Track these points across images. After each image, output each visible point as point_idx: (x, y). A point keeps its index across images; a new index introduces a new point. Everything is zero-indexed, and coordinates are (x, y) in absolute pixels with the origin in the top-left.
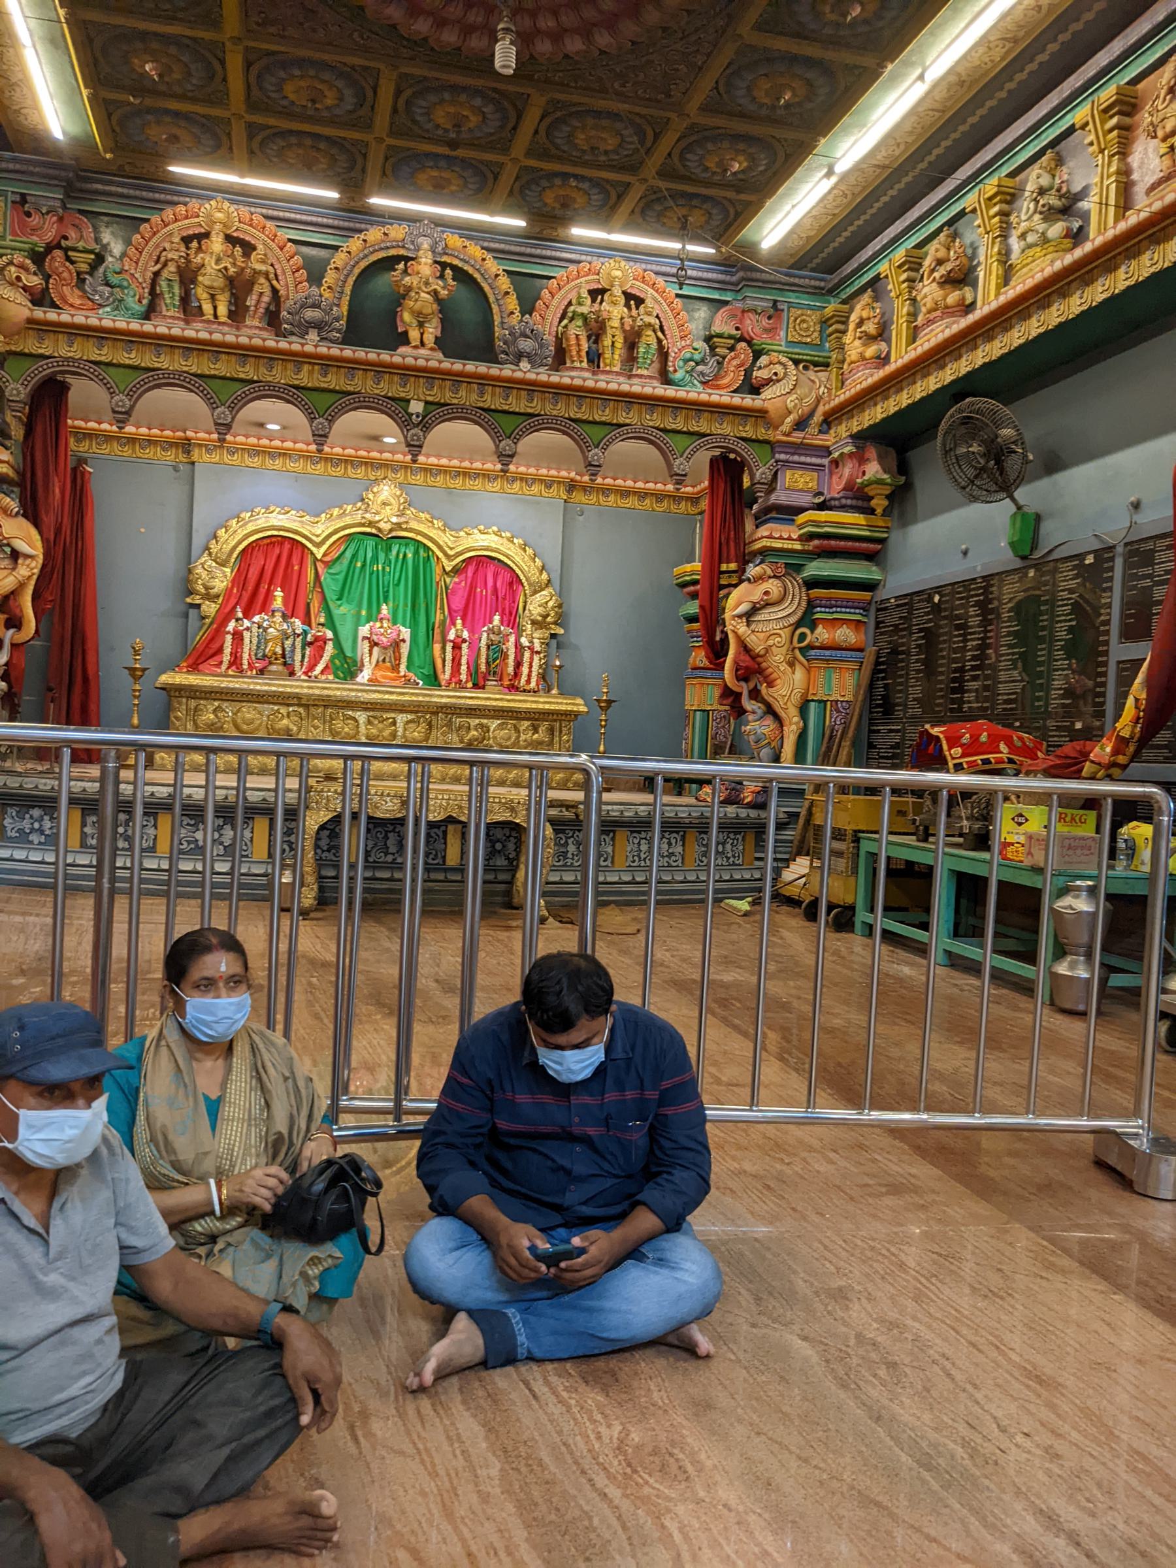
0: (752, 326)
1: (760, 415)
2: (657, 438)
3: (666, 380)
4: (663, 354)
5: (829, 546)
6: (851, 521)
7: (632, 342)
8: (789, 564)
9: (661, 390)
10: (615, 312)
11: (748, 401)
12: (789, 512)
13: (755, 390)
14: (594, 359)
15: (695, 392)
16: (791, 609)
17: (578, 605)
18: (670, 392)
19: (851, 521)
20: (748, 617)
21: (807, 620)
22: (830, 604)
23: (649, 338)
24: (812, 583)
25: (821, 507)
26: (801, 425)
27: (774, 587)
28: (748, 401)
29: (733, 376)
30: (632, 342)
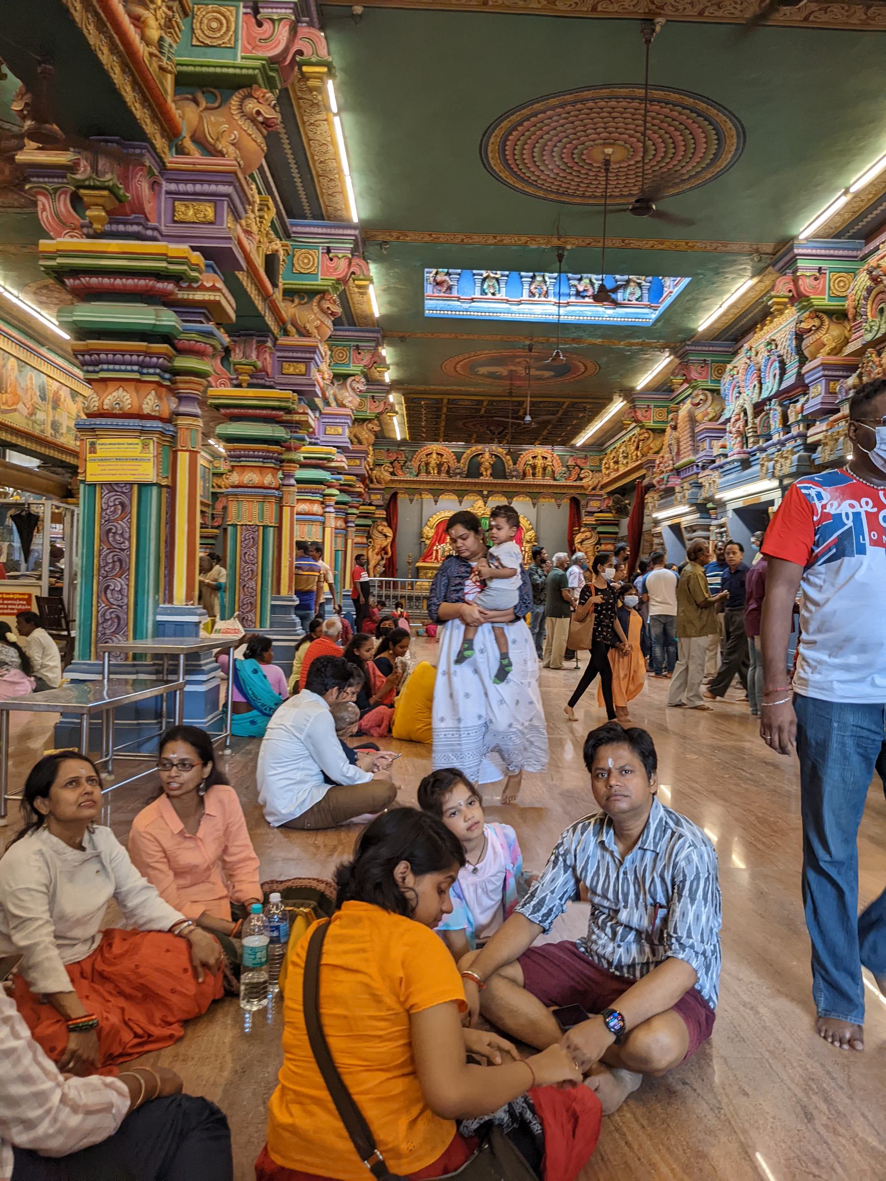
0: (579, 462)
1: (582, 487)
2: (554, 496)
3: (555, 480)
4: (553, 472)
5: (604, 523)
6: (608, 516)
7: (544, 469)
8: (593, 528)
10: (539, 462)
11: (578, 483)
12: (591, 513)
13: (581, 479)
14: (534, 475)
15: (563, 482)
16: (593, 540)
17: (542, 535)
18: (555, 483)
19: (608, 516)
20: (581, 543)
21: (599, 543)
22: (605, 538)
23: (549, 468)
24: (599, 533)
25: (601, 512)
26: (594, 489)
27: (588, 534)
28: (578, 483)
29: (574, 476)
30: (544, 469)
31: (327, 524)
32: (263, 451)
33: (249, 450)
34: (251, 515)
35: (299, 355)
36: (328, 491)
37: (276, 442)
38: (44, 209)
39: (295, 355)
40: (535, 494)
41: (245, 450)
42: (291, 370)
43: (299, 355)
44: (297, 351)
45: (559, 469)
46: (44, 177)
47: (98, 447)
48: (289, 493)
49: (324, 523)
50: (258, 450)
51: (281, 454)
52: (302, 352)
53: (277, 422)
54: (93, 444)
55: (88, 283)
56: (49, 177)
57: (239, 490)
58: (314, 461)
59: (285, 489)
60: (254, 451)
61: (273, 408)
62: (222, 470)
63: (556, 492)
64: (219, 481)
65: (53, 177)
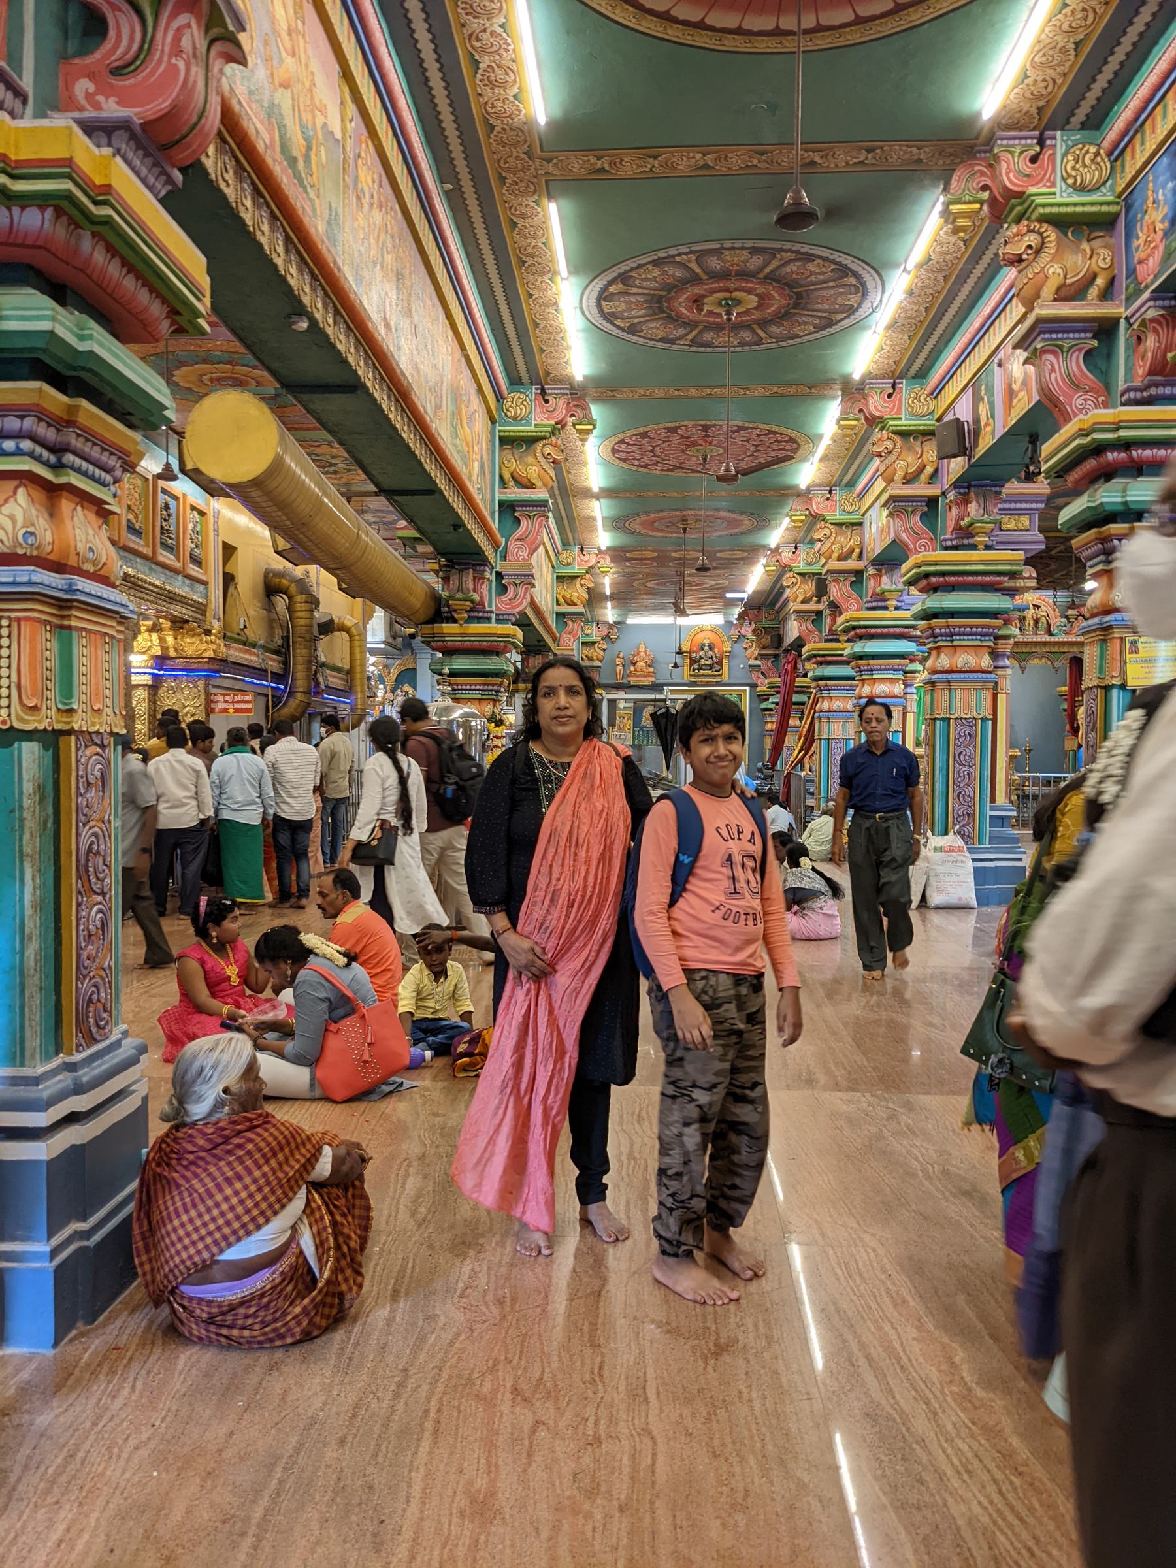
2: (1050, 656)
3: (1051, 635)
4: (1049, 625)
7: (1037, 621)
9: (1048, 638)
15: (1062, 638)
18: (1052, 639)
30: (1037, 621)
31: (909, 708)
32: (983, 626)
33: (965, 626)
34: (967, 706)
35: (1023, 505)
36: (911, 667)
37: (994, 614)
38: (1053, 370)
39: (1018, 506)
40: (1023, 653)
41: (960, 626)
42: (1012, 526)
43: (1023, 505)
44: (1020, 501)
45: (1057, 621)
46: (1057, 332)
47: (1140, 646)
48: (1004, 676)
49: (905, 707)
50: (977, 626)
51: (999, 628)
52: (1026, 501)
53: (997, 590)
54: (1134, 643)
55: (1140, 457)
56: (1063, 332)
57: (954, 675)
58: (898, 630)
59: (1000, 672)
60: (971, 627)
61: (999, 573)
62: (594, 639)
63: (1051, 650)
64: (590, 652)
65: (1068, 332)
